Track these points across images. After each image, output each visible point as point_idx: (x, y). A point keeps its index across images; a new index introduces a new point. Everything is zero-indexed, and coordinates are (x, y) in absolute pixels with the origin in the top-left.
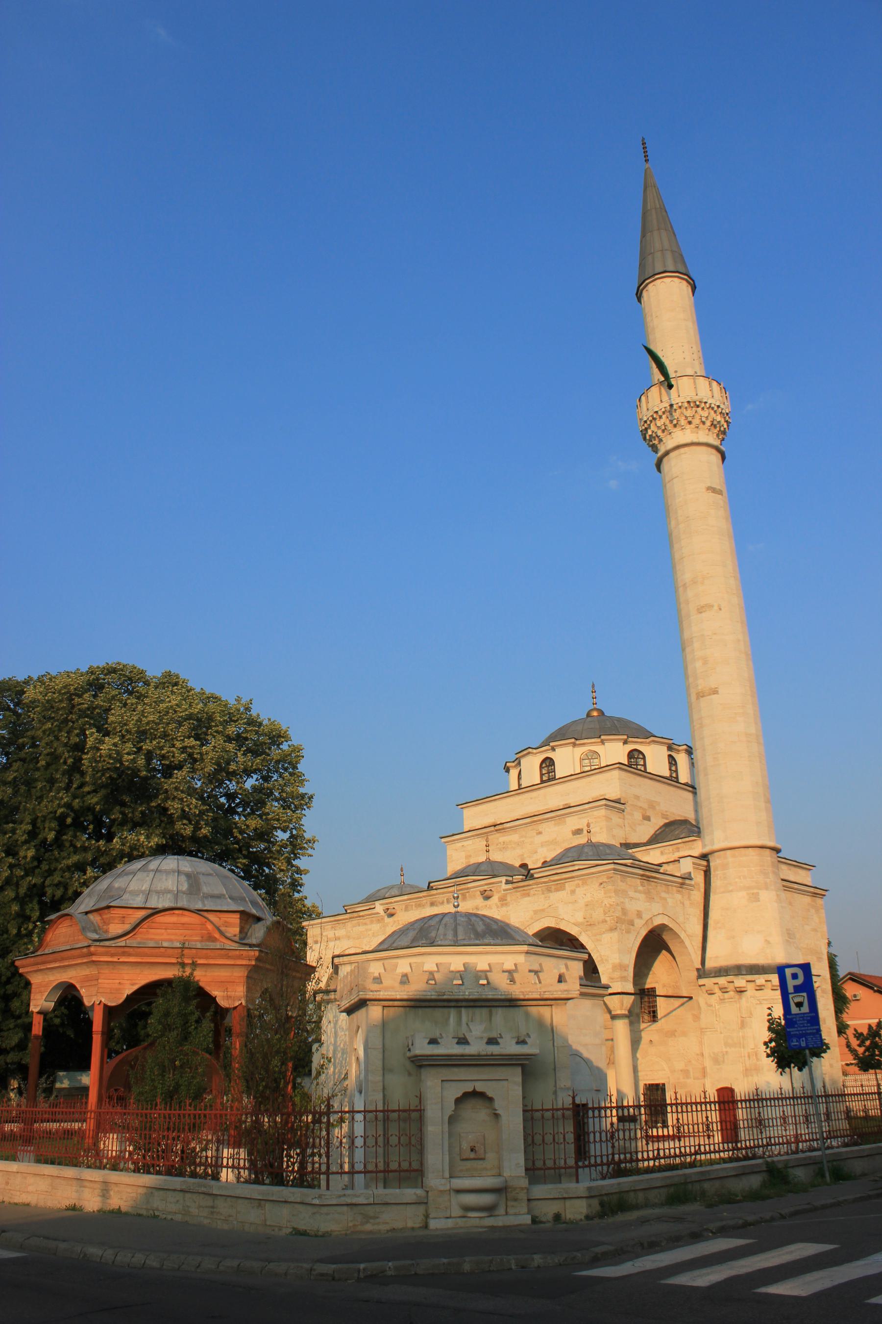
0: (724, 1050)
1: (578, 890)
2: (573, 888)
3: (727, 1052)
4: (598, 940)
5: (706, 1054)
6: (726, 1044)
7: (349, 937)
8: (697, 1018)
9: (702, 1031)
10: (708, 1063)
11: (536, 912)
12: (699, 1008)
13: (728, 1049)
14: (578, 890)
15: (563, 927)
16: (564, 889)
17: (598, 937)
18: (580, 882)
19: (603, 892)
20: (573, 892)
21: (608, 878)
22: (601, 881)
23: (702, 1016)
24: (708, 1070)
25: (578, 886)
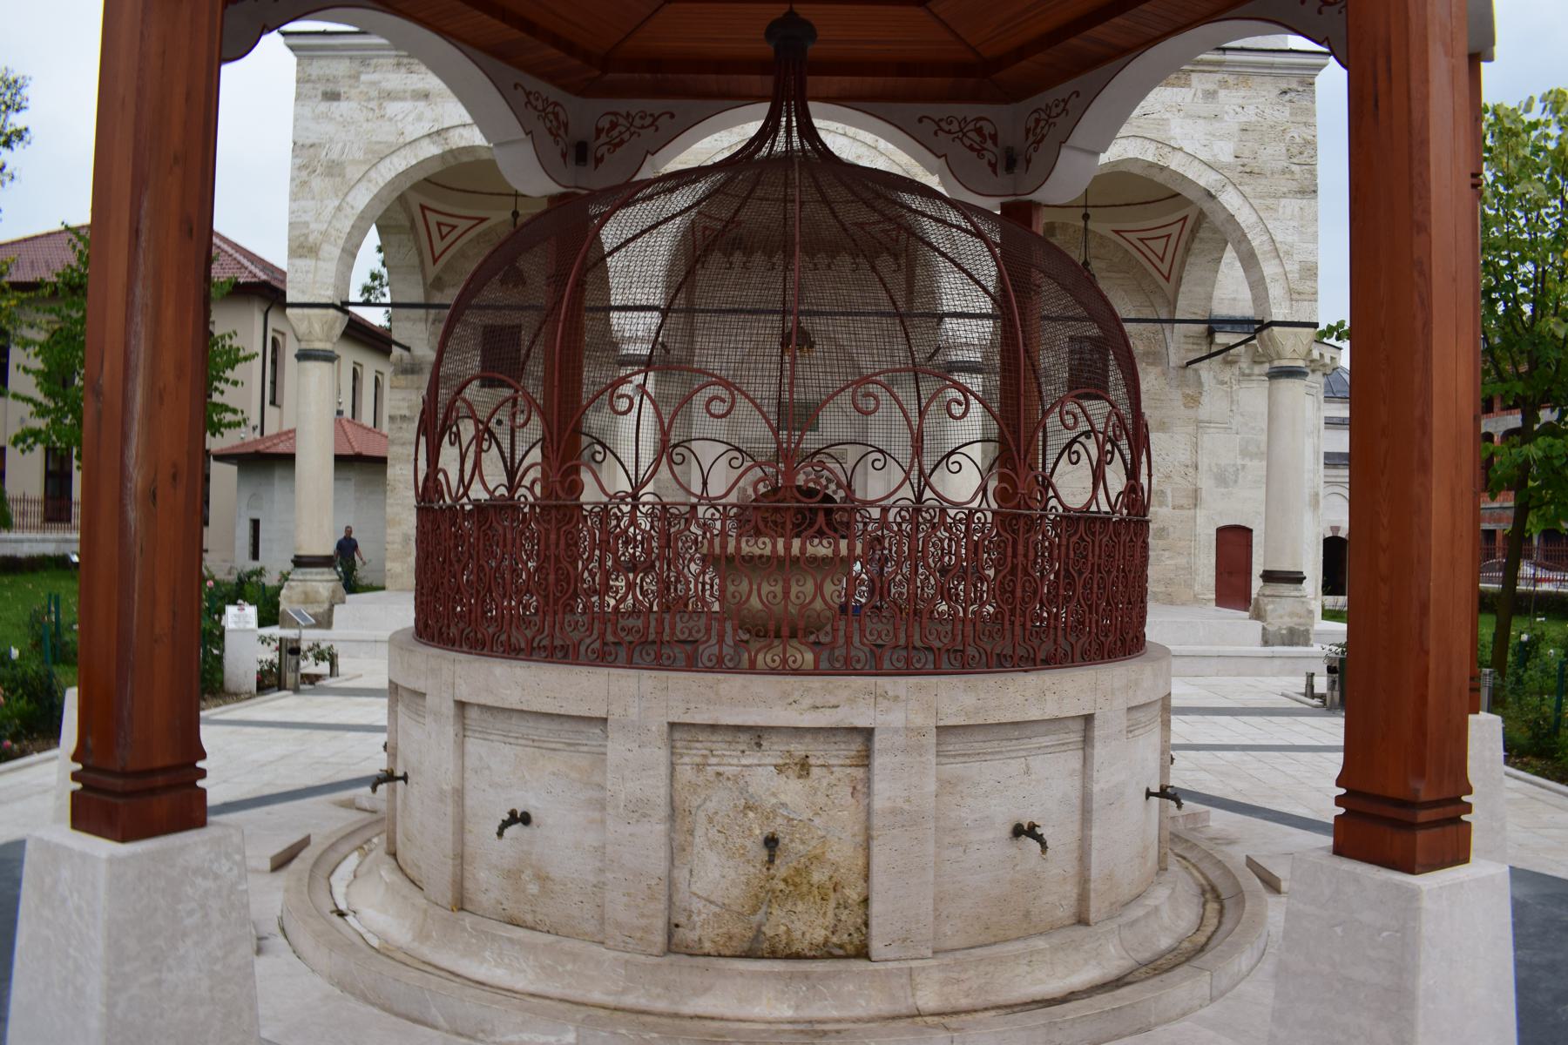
0: (1239, 462)
1: (1222, 93)
2: (1211, 87)
3: (1244, 466)
4: (1268, 208)
5: (1203, 466)
6: (1245, 453)
8: (1193, 401)
9: (1199, 424)
10: (1206, 483)
12: (1200, 384)
13: (1247, 462)
14: (1222, 93)
15: (1175, 163)
16: (1189, 86)
17: (1269, 202)
18: (1231, 79)
19: (1287, 113)
20: (1210, 95)
21: (1301, 83)
22: (1284, 86)
23: (1205, 399)
24: (1204, 494)
25: (1224, 84)
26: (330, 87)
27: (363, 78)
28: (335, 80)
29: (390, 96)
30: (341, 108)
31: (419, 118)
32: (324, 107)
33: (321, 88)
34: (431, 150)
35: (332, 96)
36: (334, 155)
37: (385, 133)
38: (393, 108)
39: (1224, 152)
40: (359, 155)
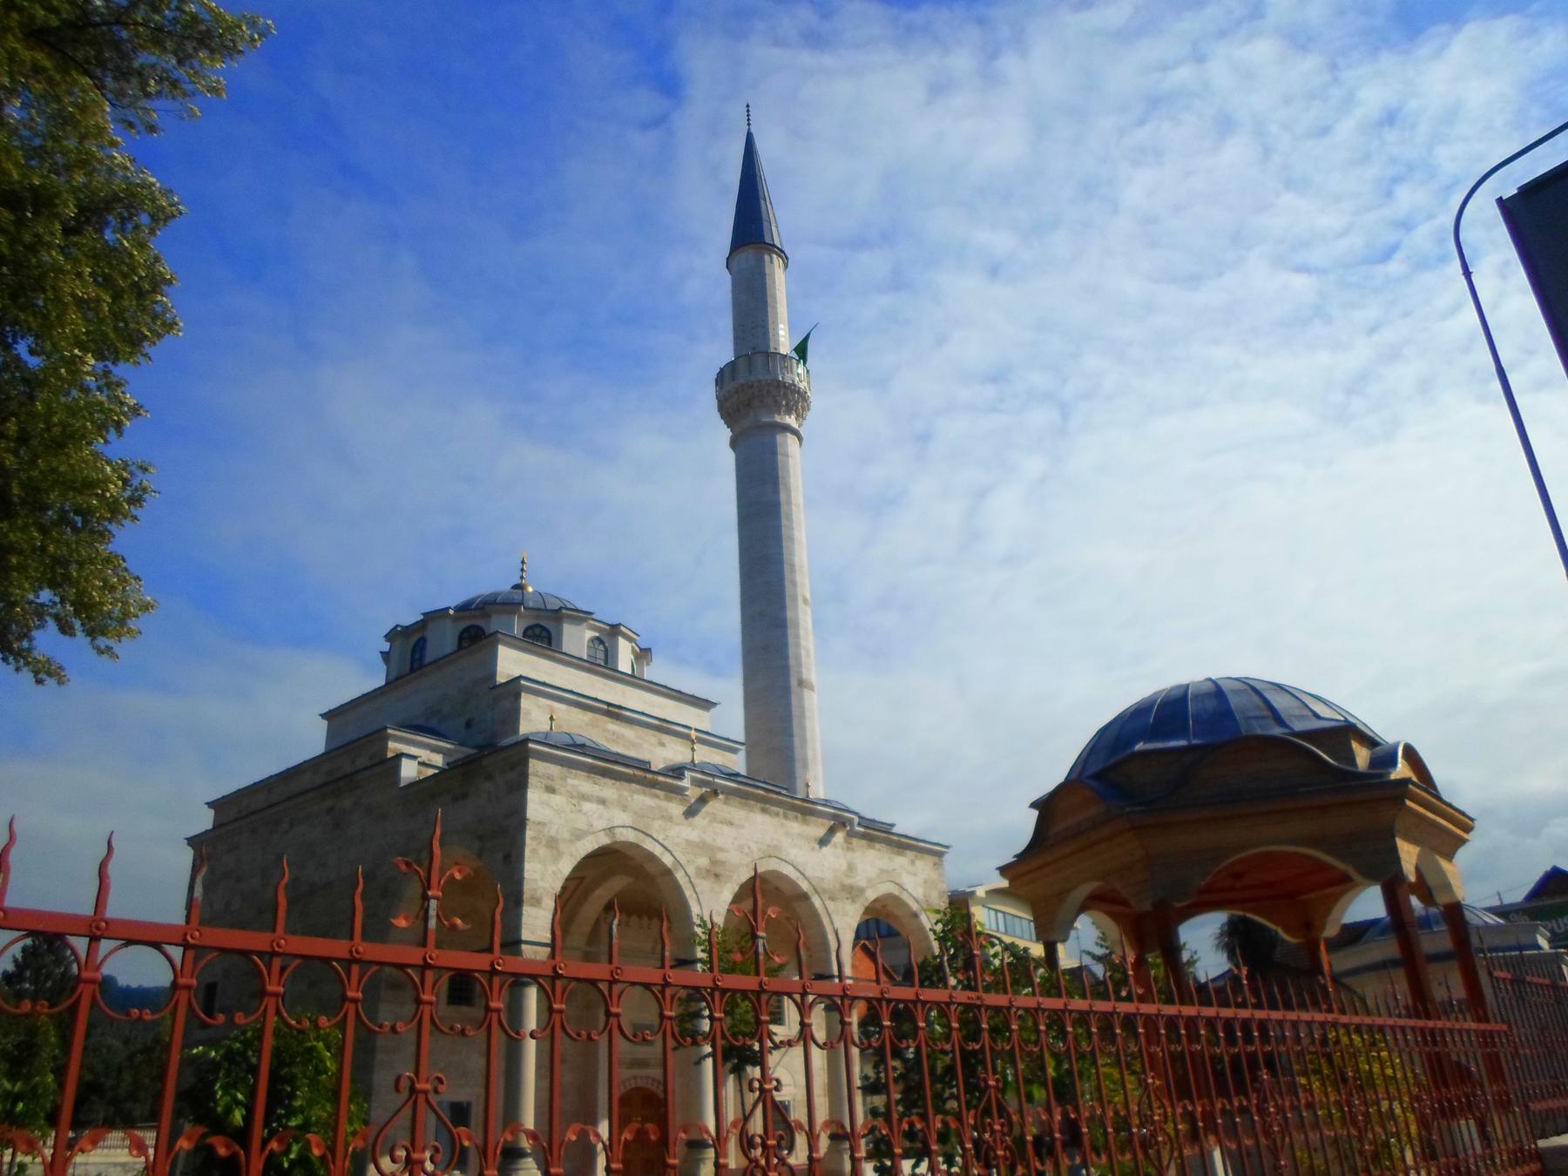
7: (625, 808)
11: (882, 871)
20: (913, 862)
26: (550, 783)
27: (570, 781)
28: (550, 778)
29: (584, 797)
30: (557, 800)
31: (600, 817)
32: (546, 796)
33: (545, 782)
34: (605, 840)
35: (551, 790)
36: (553, 833)
37: (581, 823)
38: (588, 806)
39: (919, 892)
40: (567, 835)
